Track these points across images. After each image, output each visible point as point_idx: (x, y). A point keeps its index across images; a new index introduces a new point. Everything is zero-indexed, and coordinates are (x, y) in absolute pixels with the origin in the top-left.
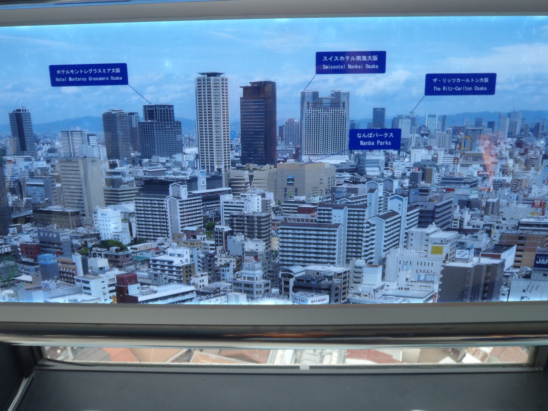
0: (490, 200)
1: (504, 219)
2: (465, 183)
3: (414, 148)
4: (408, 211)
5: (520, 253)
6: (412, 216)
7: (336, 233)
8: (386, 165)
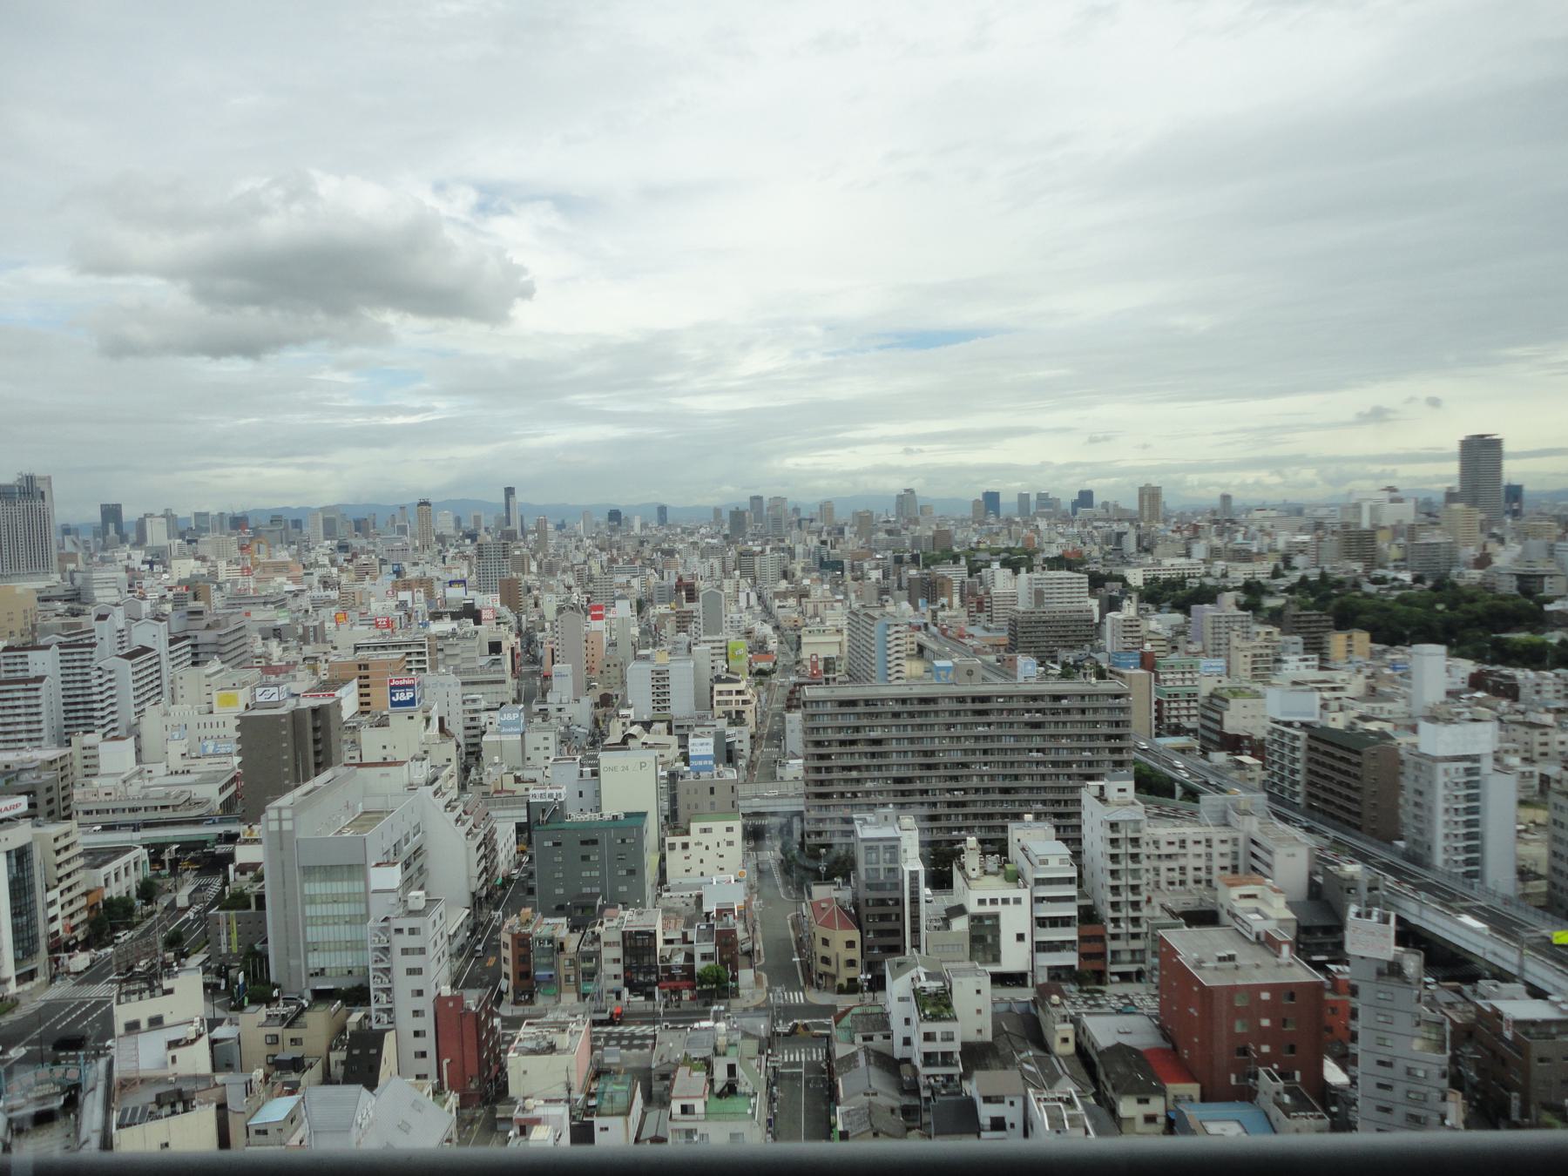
0: (309, 623)
1: (335, 648)
2: (265, 603)
3: (176, 558)
4: (172, 643)
5: (365, 691)
6: (179, 653)
7: (39, 693)
8: (130, 586)
